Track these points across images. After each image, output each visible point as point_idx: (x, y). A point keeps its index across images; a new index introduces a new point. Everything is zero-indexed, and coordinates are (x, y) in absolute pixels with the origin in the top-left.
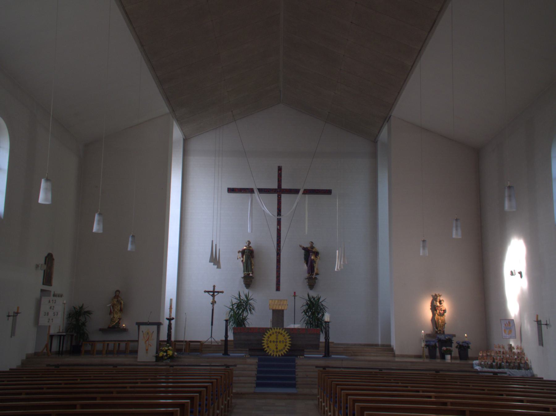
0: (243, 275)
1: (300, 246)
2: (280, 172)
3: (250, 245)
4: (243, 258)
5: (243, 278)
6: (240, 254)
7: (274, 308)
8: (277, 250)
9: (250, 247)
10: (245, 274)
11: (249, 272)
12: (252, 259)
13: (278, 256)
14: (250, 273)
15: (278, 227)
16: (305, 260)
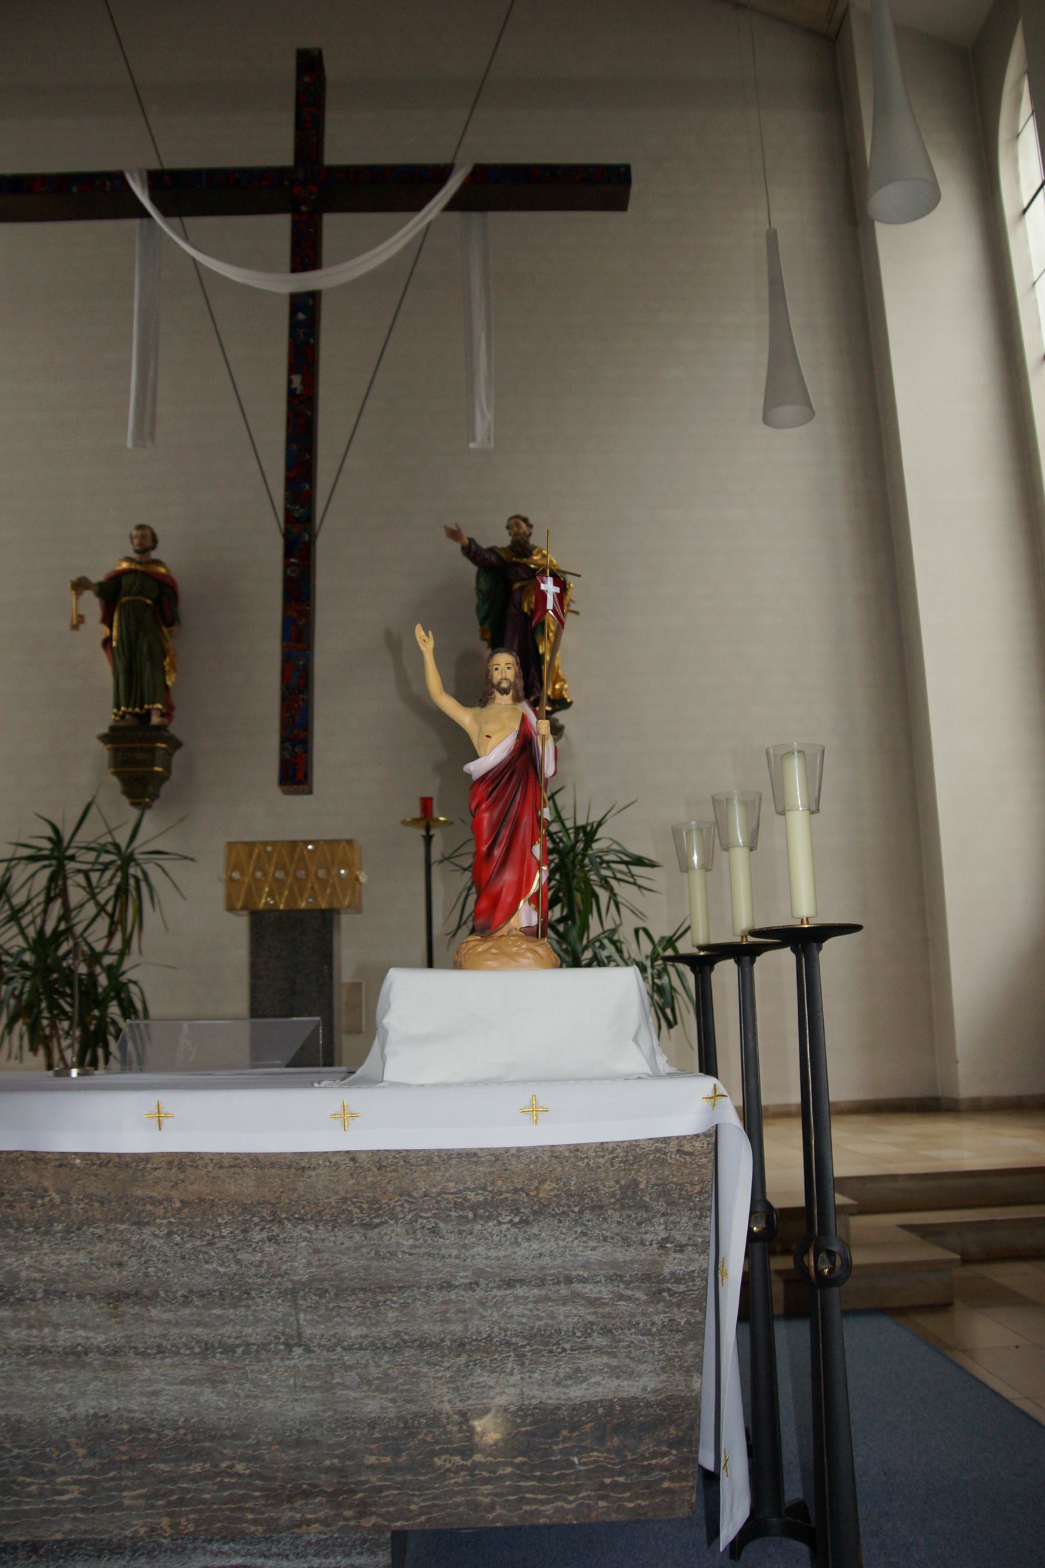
0: (105, 730)
1: (454, 534)
2: (306, 79)
3: (154, 555)
4: (111, 627)
5: (105, 738)
6: (91, 605)
7: (264, 902)
8: (289, 518)
9: (158, 562)
10: (123, 717)
11: (142, 707)
12: (164, 629)
13: (293, 560)
14: (148, 713)
15: (297, 379)
16: (482, 624)
